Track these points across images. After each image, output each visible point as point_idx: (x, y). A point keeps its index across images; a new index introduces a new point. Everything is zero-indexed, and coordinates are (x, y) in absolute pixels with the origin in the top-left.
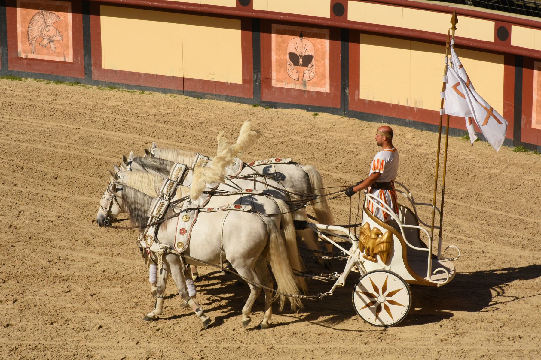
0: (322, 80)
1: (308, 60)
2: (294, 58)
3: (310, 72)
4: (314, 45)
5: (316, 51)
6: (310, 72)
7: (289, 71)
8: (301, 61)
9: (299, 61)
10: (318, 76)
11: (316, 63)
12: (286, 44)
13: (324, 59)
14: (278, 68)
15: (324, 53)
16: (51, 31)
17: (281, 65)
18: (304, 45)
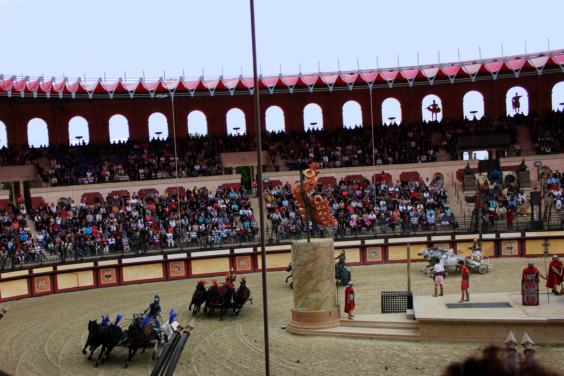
1: (110, 276)
2: (106, 276)
5: (112, 273)
16: (44, 284)
17: (103, 278)
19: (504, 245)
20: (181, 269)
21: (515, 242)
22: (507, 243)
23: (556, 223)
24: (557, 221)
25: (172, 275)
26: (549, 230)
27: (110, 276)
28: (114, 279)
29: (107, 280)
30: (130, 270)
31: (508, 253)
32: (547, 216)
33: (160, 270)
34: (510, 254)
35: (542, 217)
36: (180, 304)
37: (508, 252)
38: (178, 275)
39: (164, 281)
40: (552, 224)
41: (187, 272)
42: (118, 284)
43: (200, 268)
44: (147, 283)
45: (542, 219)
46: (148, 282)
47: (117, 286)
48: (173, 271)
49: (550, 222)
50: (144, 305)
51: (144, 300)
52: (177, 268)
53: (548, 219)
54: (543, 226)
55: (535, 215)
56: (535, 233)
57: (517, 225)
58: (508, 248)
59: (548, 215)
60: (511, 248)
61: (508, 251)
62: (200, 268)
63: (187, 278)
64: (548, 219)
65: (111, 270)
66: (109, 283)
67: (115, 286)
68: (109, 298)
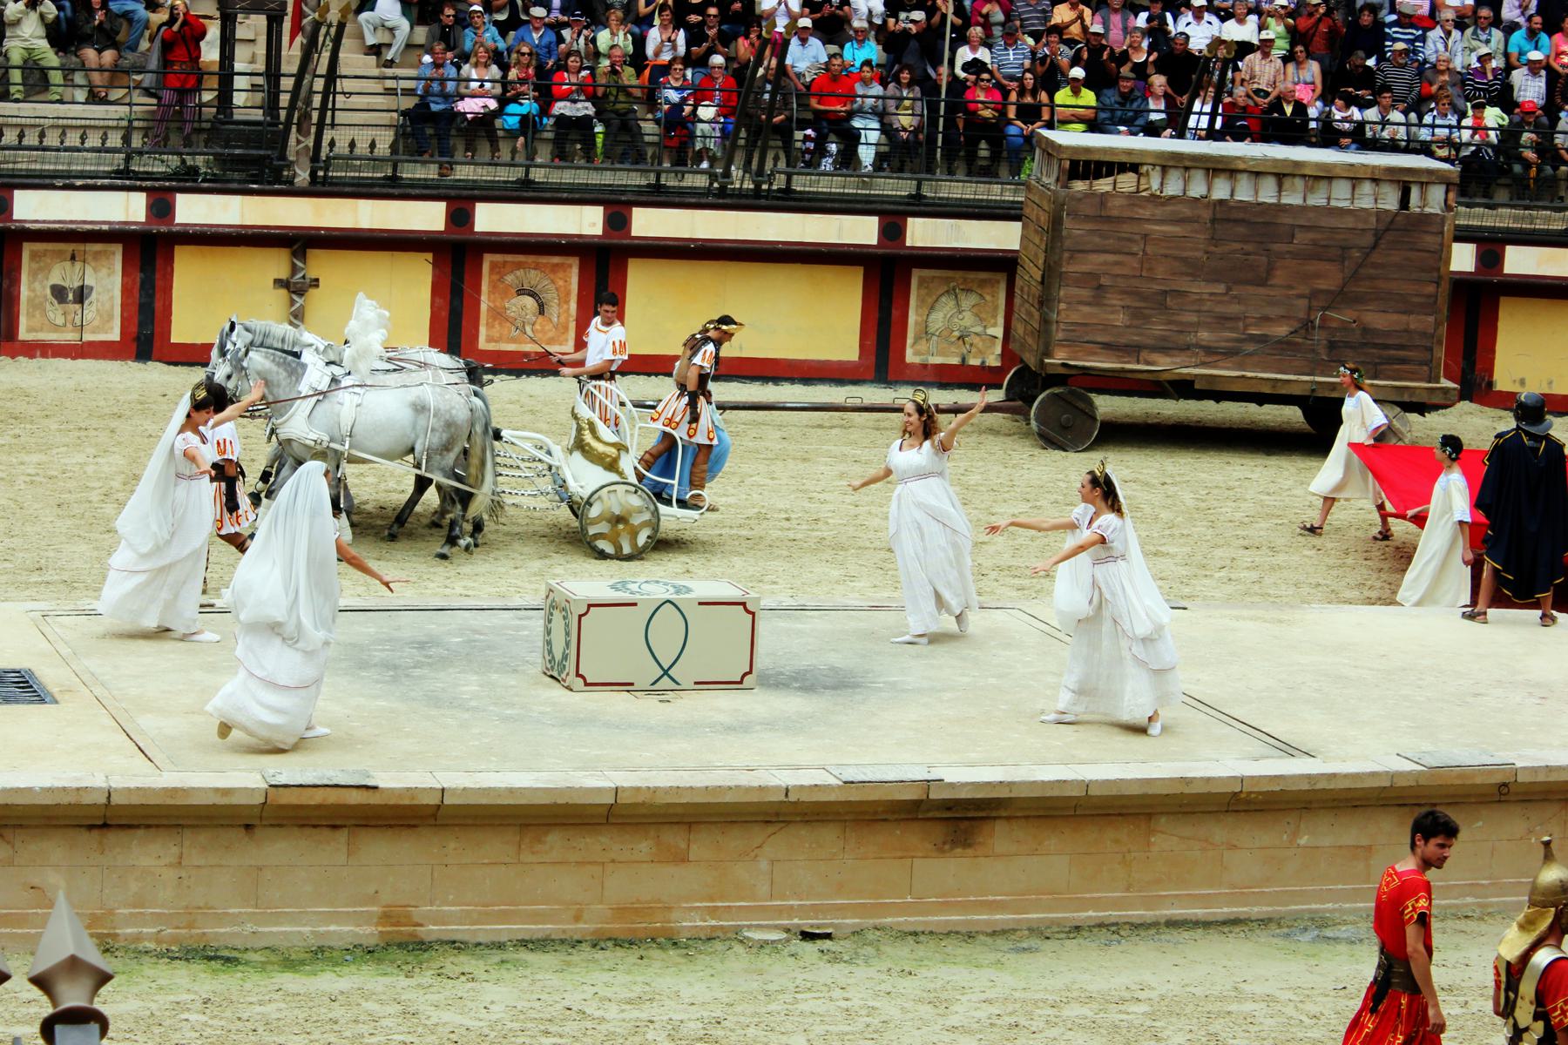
19: (34, 274)
21: (108, 255)
22: (60, 253)
23: (362, 148)
24: (369, 133)
26: (321, 188)
31: (56, 328)
32: (311, 92)
34: (70, 337)
35: (284, 99)
37: (60, 320)
40: (342, 147)
45: (283, 114)
49: (328, 135)
53: (315, 116)
54: (283, 157)
55: (240, 82)
56: (236, 201)
57: (126, 139)
58: (59, 293)
59: (319, 84)
60: (81, 295)
61: (56, 313)
64: (315, 116)
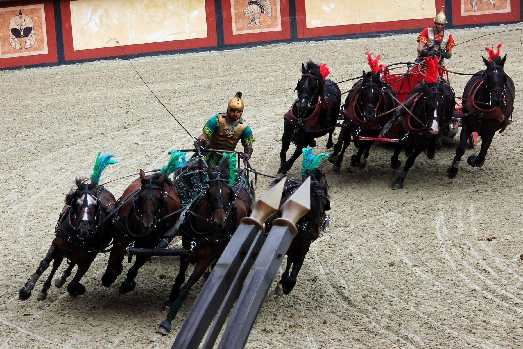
0: (41, 44)
1: (27, 31)
2: (16, 32)
3: (30, 40)
4: (32, 18)
5: (34, 23)
6: (30, 40)
7: (13, 44)
8: (22, 34)
9: (20, 34)
10: (38, 42)
11: (35, 32)
12: (8, 22)
13: (41, 28)
14: (3, 43)
15: (41, 23)
18: (23, 20)
20: (268, 10)
25: (238, 29)
27: (27, 31)
28: (42, 41)
29: (18, 47)
30: (94, 11)
33: (195, 13)
36: (265, 129)
38: (258, 31)
39: (209, 49)
41: (288, 19)
42: (55, 58)
43: (332, 6)
44: (151, 54)
46: (157, 53)
47: (51, 65)
48: (240, 16)
50: (142, 131)
51: (143, 115)
52: (256, 7)
62: (332, 6)
63: (289, 41)
65: (32, 11)
66: (24, 54)
67: (43, 65)
68: (24, 106)
